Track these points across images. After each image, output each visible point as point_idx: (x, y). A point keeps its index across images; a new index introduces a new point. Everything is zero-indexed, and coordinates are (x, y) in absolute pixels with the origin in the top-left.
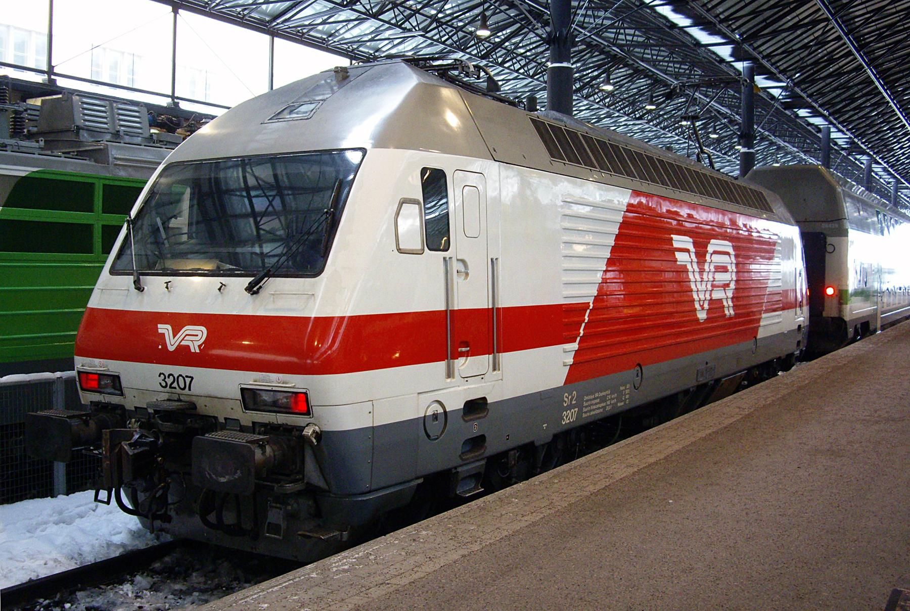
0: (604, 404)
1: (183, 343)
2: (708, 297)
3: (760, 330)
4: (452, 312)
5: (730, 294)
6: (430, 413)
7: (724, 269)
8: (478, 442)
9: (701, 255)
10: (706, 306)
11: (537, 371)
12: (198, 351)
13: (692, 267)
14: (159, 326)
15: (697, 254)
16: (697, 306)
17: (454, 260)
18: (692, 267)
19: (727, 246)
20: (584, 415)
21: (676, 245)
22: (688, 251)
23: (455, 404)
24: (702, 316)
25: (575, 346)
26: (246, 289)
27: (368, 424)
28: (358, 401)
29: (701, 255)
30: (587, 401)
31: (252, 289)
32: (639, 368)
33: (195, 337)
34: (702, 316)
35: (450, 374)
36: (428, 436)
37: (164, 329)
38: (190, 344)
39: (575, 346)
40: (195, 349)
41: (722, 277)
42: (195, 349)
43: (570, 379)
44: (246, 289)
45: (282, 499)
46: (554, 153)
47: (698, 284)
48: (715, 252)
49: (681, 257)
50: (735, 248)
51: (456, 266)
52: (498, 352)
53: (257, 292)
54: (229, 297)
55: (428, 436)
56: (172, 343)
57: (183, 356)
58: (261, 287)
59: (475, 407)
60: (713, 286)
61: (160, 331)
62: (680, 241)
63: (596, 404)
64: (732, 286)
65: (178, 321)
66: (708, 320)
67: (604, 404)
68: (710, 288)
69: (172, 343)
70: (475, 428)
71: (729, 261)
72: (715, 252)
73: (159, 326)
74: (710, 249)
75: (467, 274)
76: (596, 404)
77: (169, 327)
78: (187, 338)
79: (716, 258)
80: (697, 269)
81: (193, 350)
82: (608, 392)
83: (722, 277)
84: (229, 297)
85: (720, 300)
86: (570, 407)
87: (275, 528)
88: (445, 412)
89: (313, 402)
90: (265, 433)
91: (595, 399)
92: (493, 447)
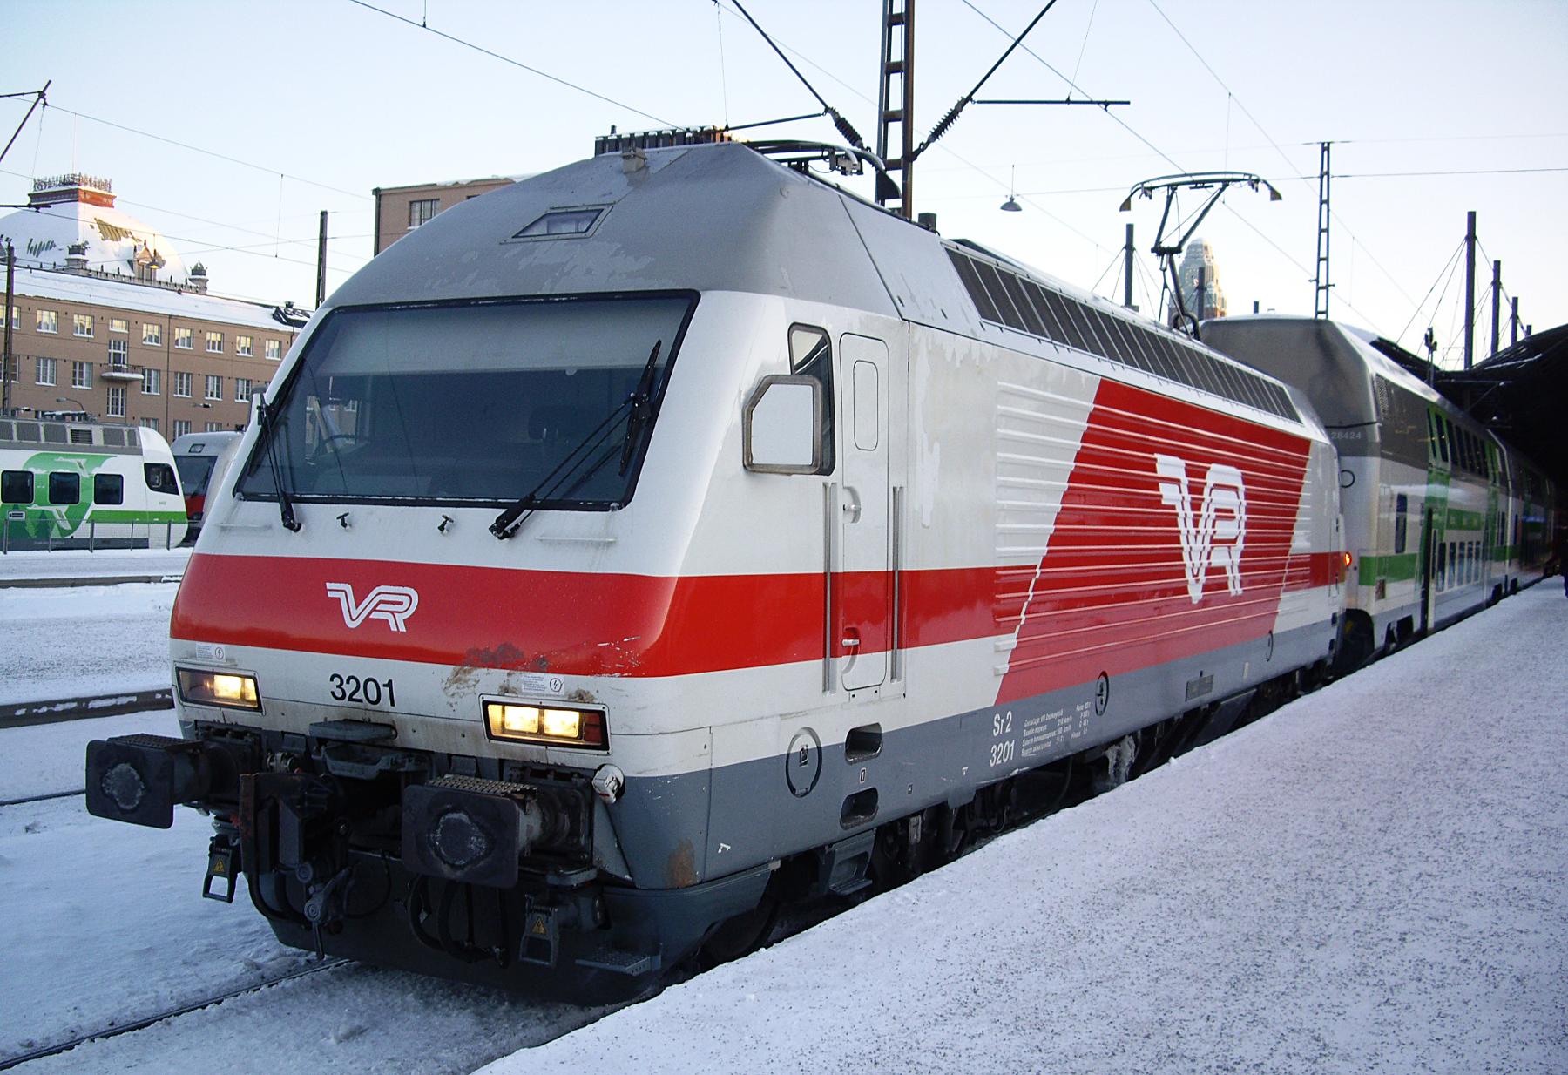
0: (1053, 734)
1: (374, 615)
2: (1206, 563)
3: (1278, 619)
4: (835, 575)
5: (1237, 560)
6: (796, 749)
8: (863, 802)
11: (948, 681)
12: (403, 629)
13: (1184, 513)
14: (329, 585)
15: (1192, 490)
17: (840, 487)
18: (1184, 513)
19: (1233, 475)
20: (1024, 754)
21: (1161, 471)
22: (1177, 481)
23: (834, 735)
25: (1010, 641)
26: (492, 529)
27: (703, 765)
28: (693, 727)
30: (1029, 728)
31: (503, 529)
32: (1103, 679)
33: (397, 607)
35: (827, 685)
36: (793, 790)
37: (340, 590)
38: (389, 617)
39: (1010, 641)
40: (398, 624)
41: (1226, 529)
42: (398, 624)
43: (1003, 696)
44: (492, 529)
45: (558, 896)
46: (986, 312)
48: (1217, 486)
49: (1168, 493)
50: (1245, 482)
51: (843, 499)
52: (900, 647)
53: (510, 535)
54: (466, 539)
55: (793, 790)
56: (353, 616)
57: (374, 642)
58: (517, 526)
59: (863, 741)
60: (1213, 541)
61: (330, 594)
62: (1169, 466)
63: (1042, 733)
64: (1240, 545)
65: (366, 575)
67: (1053, 734)
68: (1208, 546)
69: (353, 616)
70: (859, 775)
71: (1236, 502)
72: (1217, 486)
73: (329, 585)
74: (1210, 479)
75: (857, 513)
76: (1042, 733)
77: (348, 588)
78: (381, 607)
81: (394, 628)
82: (1058, 714)
83: (1226, 529)
84: (466, 539)
85: (1221, 570)
86: (1003, 738)
87: (539, 947)
88: (819, 749)
89: (612, 725)
90: (521, 780)
91: (1040, 724)
92: (887, 808)
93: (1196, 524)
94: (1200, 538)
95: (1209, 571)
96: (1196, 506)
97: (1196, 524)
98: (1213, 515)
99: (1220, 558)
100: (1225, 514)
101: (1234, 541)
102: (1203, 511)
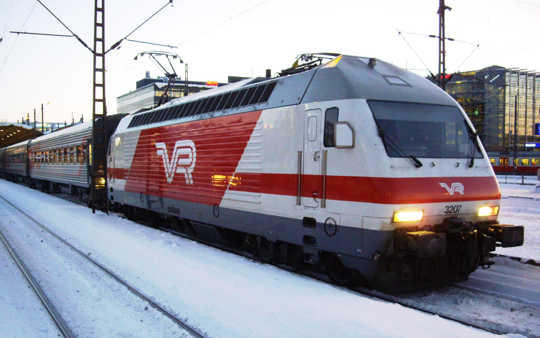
7: (187, 156)
9: (170, 150)
10: (173, 175)
16: (167, 175)
24: (170, 180)
29: (170, 150)
34: (170, 180)
47: (168, 165)
60: (177, 165)
64: (193, 166)
66: (173, 183)
68: (175, 165)
72: (178, 148)
74: (177, 145)
79: (179, 150)
80: (167, 156)
83: (182, 161)
85: (183, 175)
93: (170, 159)
94: (172, 165)
95: (176, 174)
96: (170, 155)
97: (170, 159)
98: (177, 156)
99: (180, 170)
100: (187, 156)
101: (190, 165)
102: (174, 155)
